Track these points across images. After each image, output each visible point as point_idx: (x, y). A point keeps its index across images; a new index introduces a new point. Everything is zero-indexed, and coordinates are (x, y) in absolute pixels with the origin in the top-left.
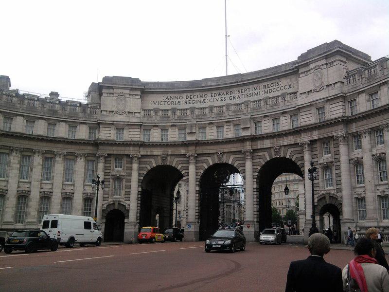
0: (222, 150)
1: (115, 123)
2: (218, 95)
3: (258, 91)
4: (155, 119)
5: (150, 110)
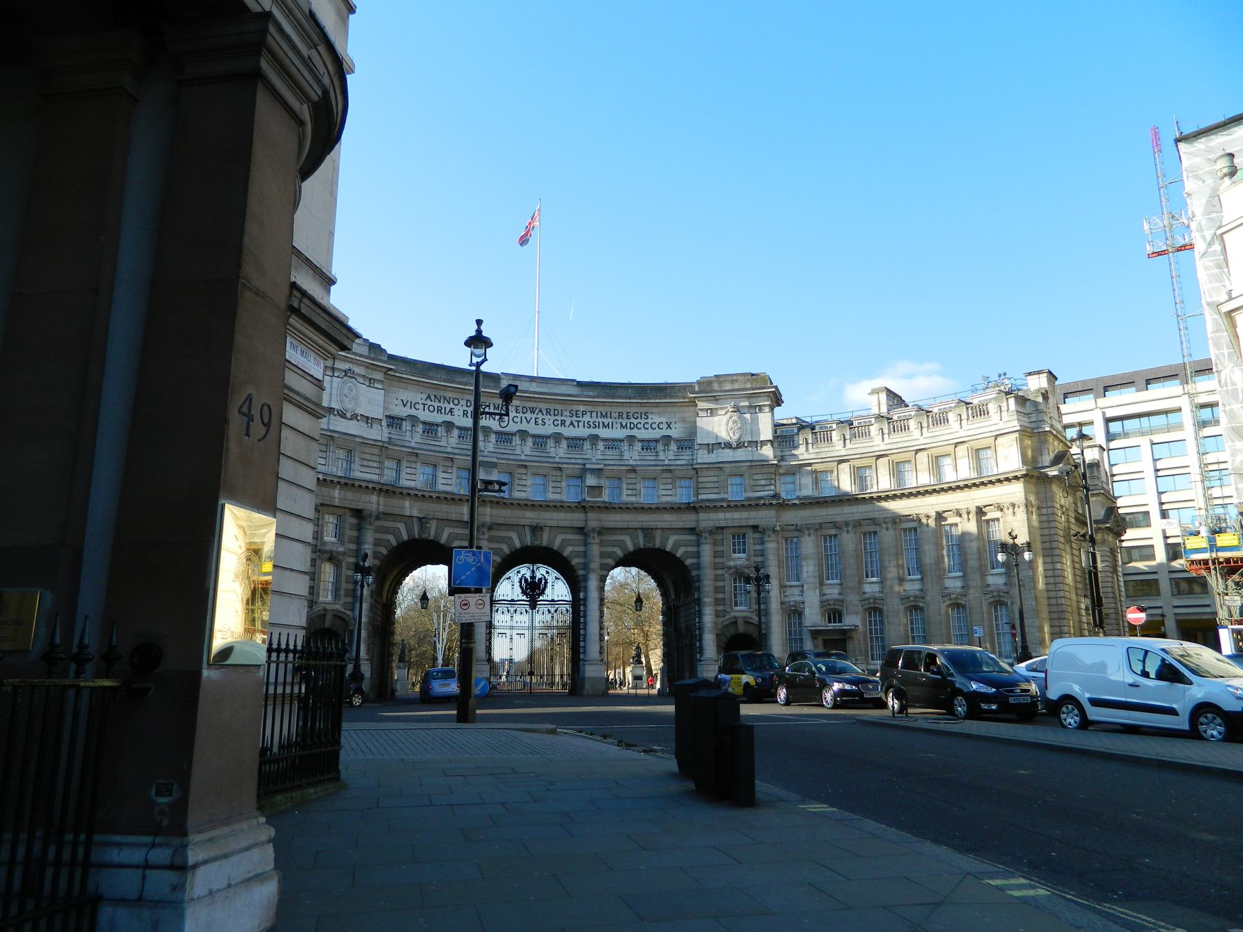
0: (541, 523)
1: (336, 435)
2: (529, 411)
3: (611, 421)
4: (414, 438)
5: (402, 419)
